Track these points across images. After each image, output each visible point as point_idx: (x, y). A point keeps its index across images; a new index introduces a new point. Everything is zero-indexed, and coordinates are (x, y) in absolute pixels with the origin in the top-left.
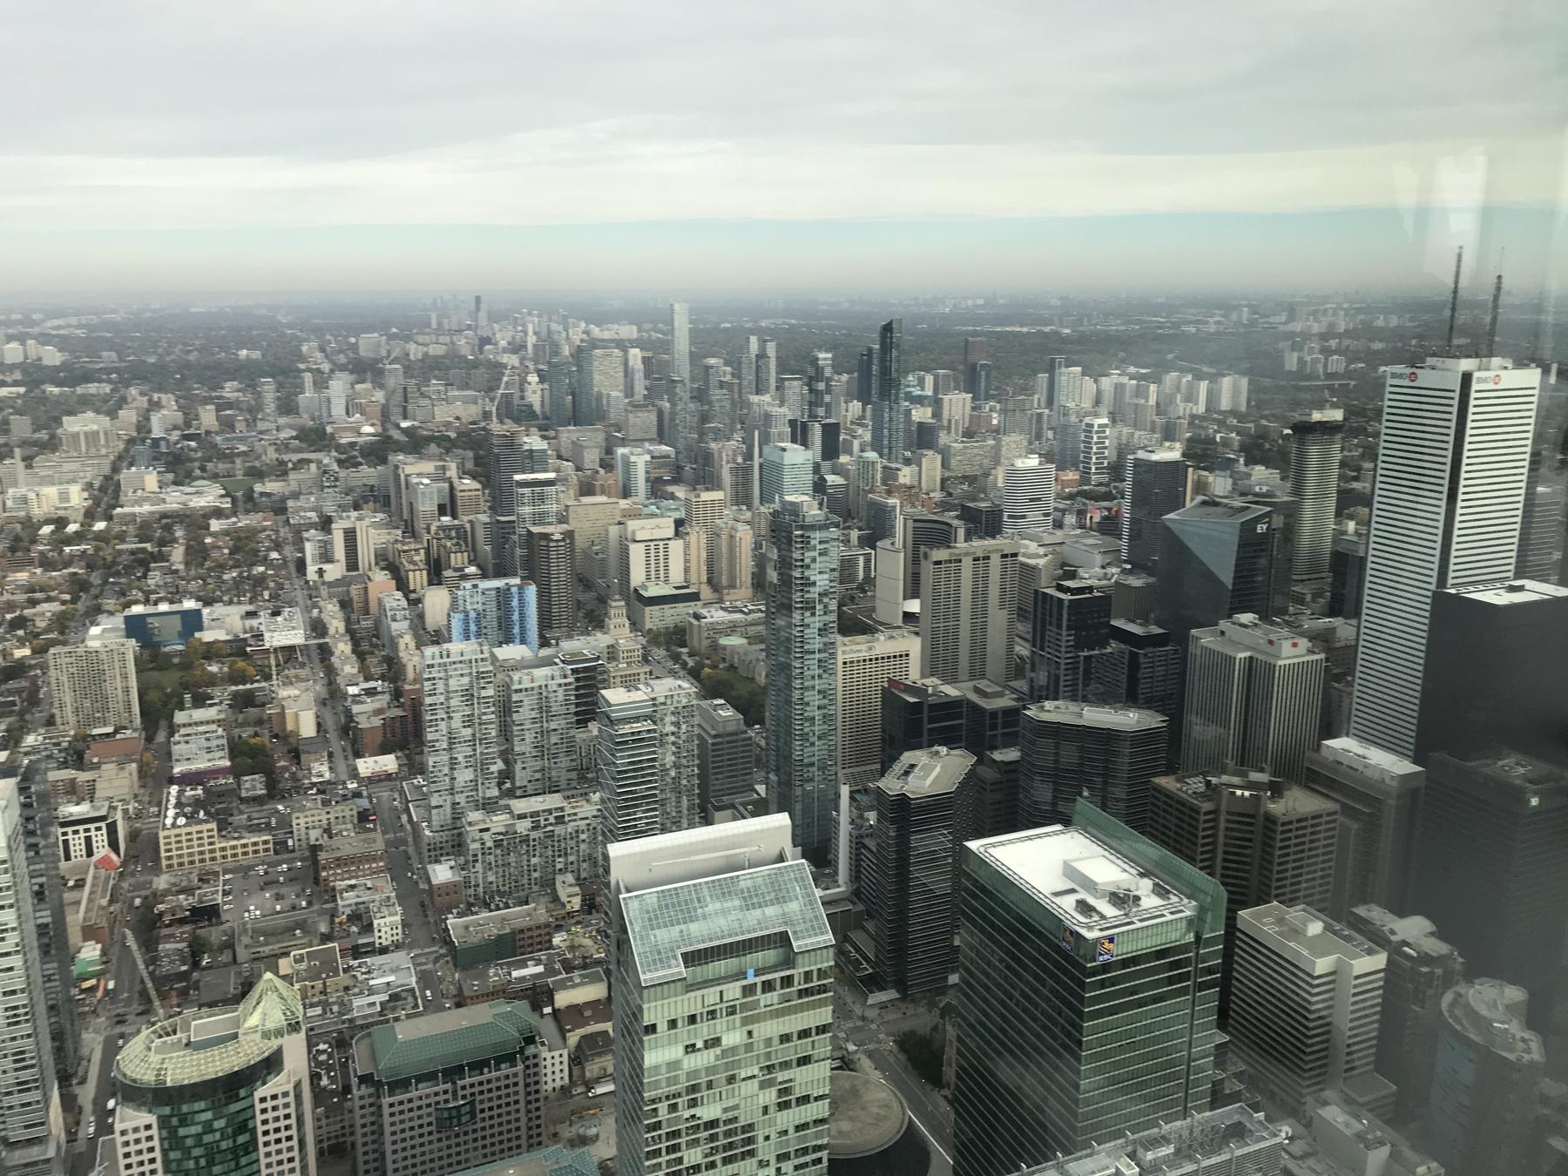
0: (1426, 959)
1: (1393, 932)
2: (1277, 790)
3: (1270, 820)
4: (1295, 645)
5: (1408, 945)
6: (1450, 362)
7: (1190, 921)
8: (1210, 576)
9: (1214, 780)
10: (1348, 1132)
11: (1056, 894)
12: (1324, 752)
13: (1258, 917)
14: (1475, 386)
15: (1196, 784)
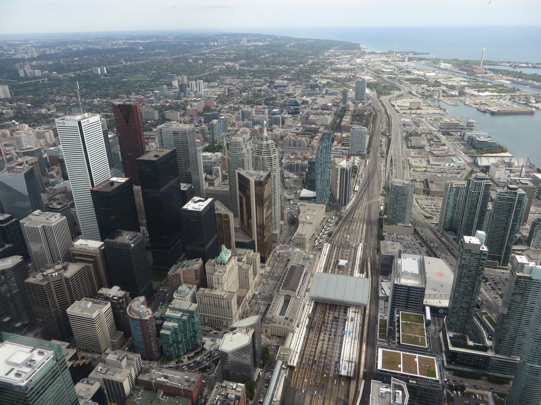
0: (120, 298)
1: (110, 295)
2: (65, 268)
3: (67, 279)
4: (55, 217)
5: (114, 296)
6: (73, 117)
7: (53, 358)
8: (20, 194)
9: (45, 273)
10: (115, 360)
11: (7, 374)
12: (75, 247)
13: (73, 308)
14: (83, 125)
15: (39, 277)
